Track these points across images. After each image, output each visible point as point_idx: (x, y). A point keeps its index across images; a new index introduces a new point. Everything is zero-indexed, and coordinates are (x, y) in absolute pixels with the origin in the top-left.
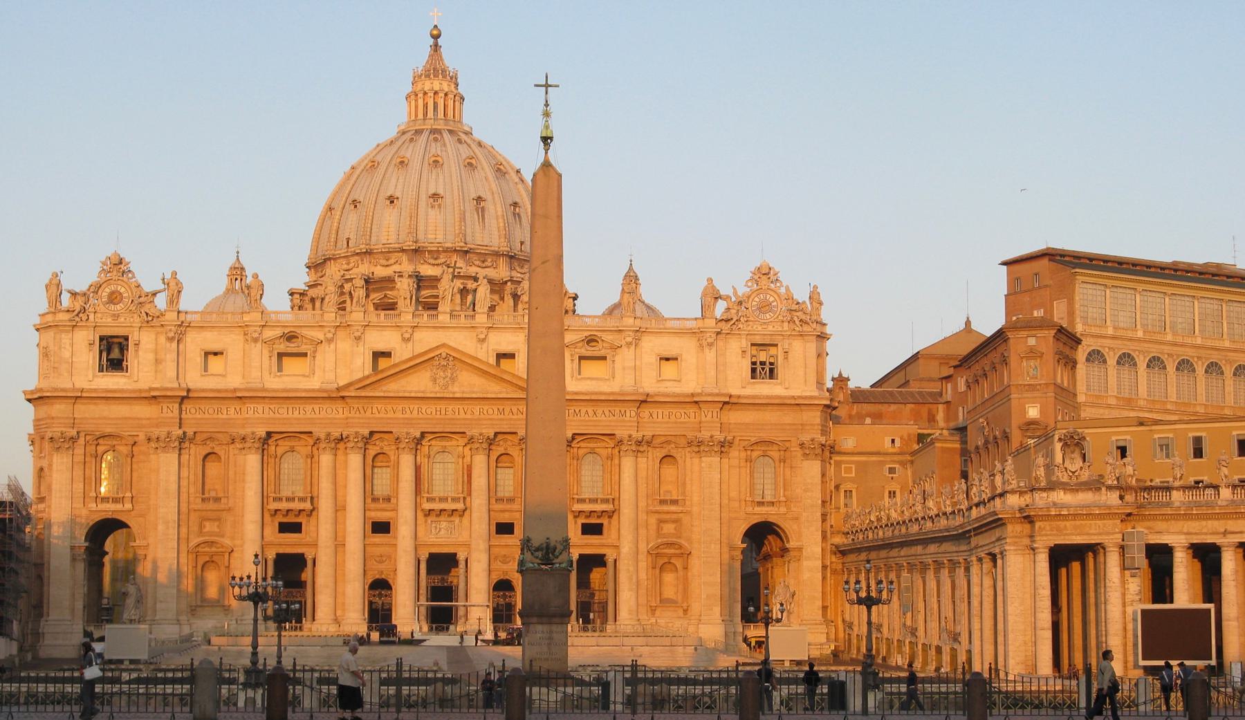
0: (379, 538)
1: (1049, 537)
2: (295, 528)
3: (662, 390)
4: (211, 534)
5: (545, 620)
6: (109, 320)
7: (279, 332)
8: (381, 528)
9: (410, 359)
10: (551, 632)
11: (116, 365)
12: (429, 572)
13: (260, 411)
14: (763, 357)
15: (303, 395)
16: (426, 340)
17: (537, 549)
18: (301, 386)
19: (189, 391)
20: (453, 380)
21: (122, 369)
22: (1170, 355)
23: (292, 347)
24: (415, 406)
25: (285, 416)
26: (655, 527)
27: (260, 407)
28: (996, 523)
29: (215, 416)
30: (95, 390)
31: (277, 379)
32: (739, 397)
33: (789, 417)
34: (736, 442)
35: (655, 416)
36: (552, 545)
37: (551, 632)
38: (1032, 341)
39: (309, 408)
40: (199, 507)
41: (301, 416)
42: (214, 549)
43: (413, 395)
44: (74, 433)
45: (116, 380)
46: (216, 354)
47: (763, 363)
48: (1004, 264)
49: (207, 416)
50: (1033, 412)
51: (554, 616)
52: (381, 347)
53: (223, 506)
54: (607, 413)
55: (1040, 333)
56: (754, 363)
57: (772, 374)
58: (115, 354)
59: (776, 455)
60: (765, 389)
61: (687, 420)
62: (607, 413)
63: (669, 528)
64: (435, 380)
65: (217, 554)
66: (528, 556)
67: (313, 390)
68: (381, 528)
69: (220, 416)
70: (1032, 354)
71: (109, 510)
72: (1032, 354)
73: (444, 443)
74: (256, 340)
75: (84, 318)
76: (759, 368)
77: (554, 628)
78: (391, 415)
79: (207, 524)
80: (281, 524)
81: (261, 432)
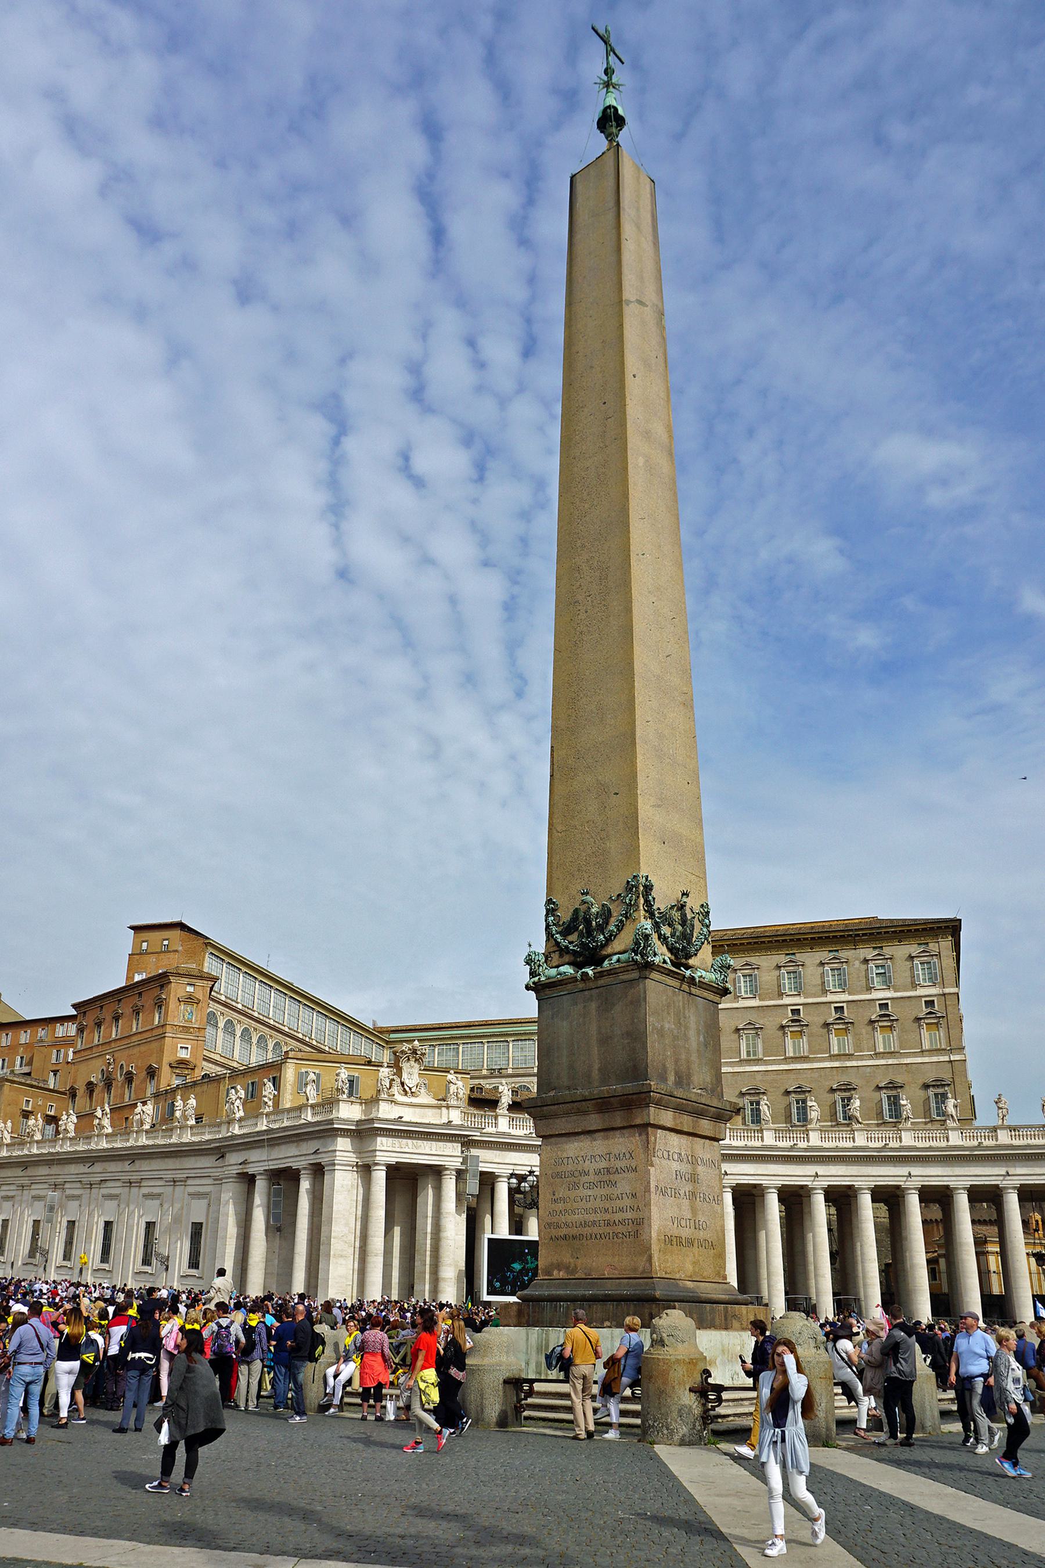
1: (389, 1151)
22: (255, 1029)
28: (327, 1132)
37: (693, 1161)
38: (190, 989)
48: (132, 928)
50: (183, 1055)
55: (199, 983)
70: (190, 1000)
72: (190, 1000)
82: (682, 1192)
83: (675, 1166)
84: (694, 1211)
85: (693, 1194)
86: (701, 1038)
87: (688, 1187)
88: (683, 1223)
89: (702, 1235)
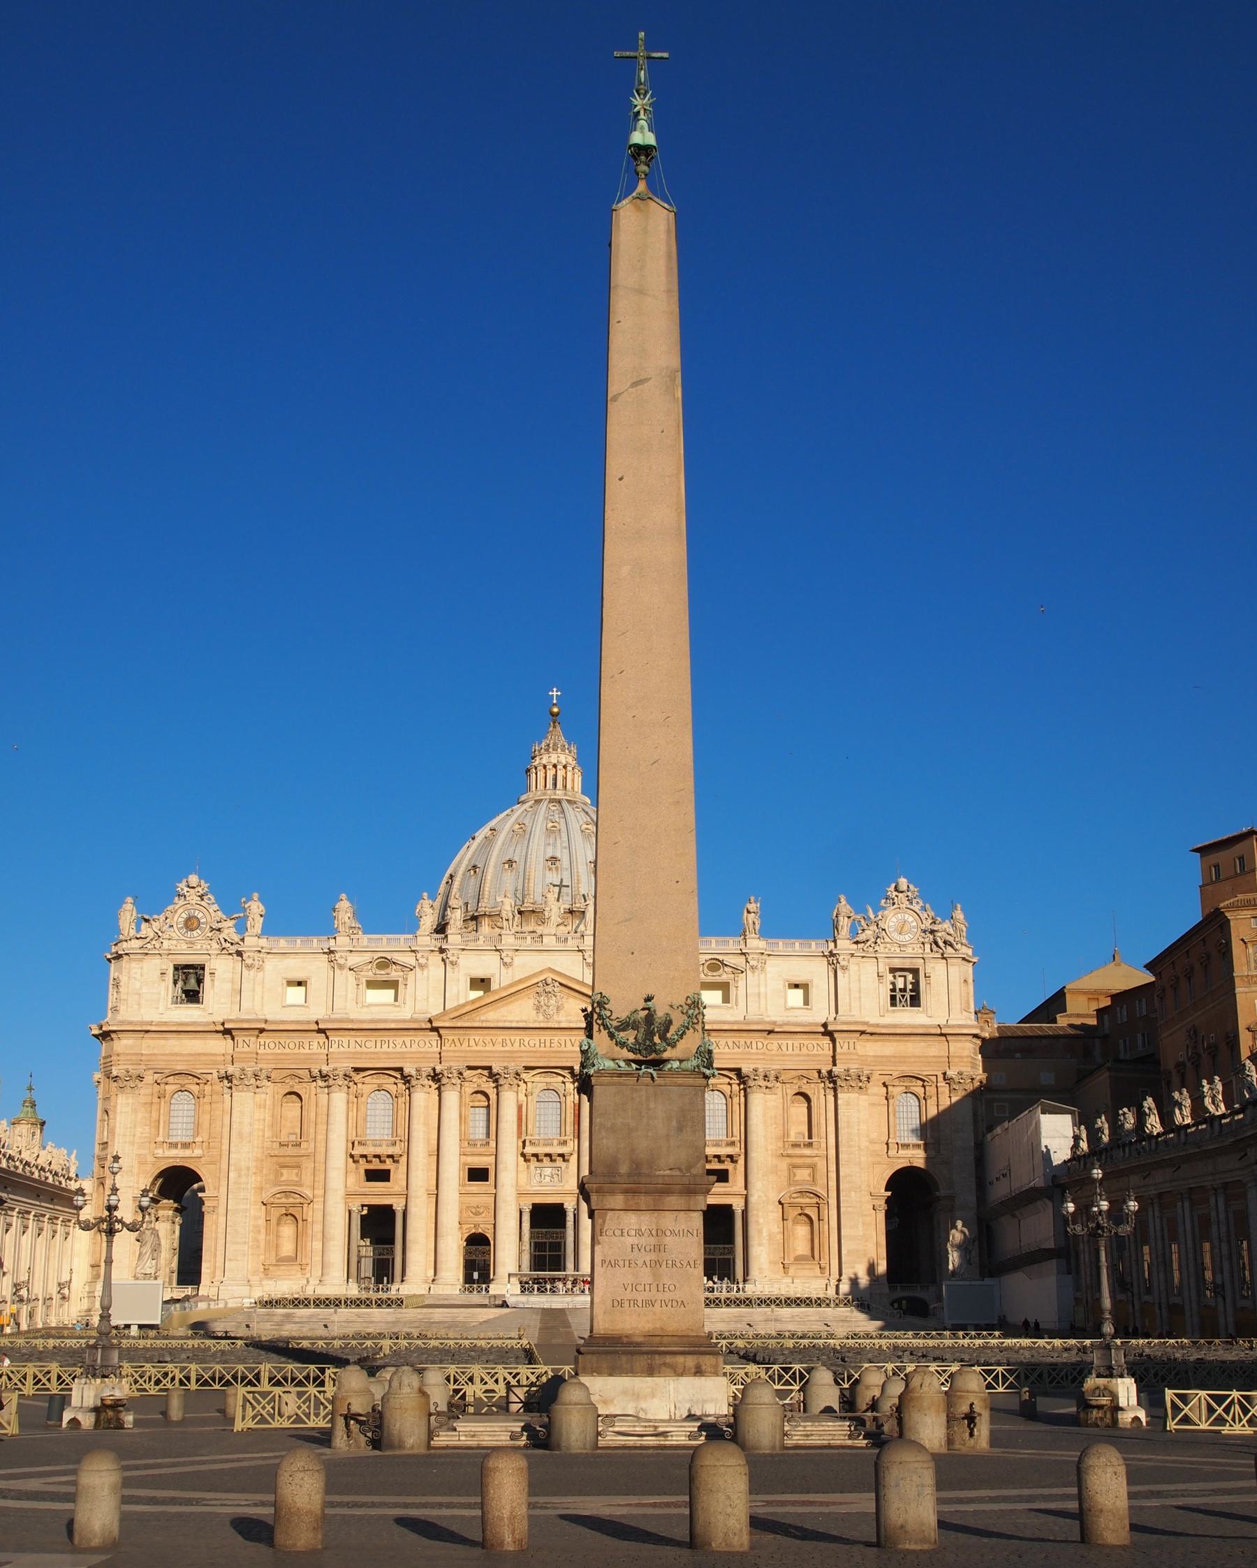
0: (477, 1186)
2: (383, 1176)
3: (792, 1019)
4: (288, 1183)
5: (643, 1200)
6: (185, 947)
7: (367, 957)
8: (478, 1174)
9: (511, 985)
10: (660, 1233)
11: (192, 996)
12: (532, 1226)
13: (346, 1045)
14: (900, 984)
15: (393, 1026)
16: (528, 964)
17: (625, 1026)
18: (391, 1016)
19: (266, 1021)
20: (558, 1009)
21: (198, 1002)
23: (382, 975)
24: (516, 1037)
25: (373, 1050)
26: (786, 1173)
27: (345, 1040)
29: (296, 1051)
30: (165, 1023)
31: (365, 1010)
32: (877, 1026)
33: (936, 1048)
34: (875, 1077)
35: (784, 1048)
36: (660, 1014)
37: (660, 1233)
39: (399, 1041)
40: (276, 1153)
41: (391, 1049)
42: (291, 1200)
43: (514, 1025)
44: (140, 1069)
45: (190, 1012)
46: (299, 984)
47: (903, 990)
49: (287, 1051)
51: (666, 1191)
52: (480, 973)
53: (302, 1152)
54: (731, 1044)
56: (893, 990)
57: (915, 1001)
58: (192, 984)
59: (920, 1091)
60: (906, 1017)
61: (821, 1052)
62: (731, 1044)
63: (803, 1174)
64: (538, 1008)
65: (294, 1205)
66: (601, 1041)
67: (404, 1021)
68: (478, 1174)
69: (302, 1050)
71: (176, 1157)
73: (548, 1080)
74: (341, 967)
75: (158, 946)
76: (898, 996)
77: (668, 1221)
78: (489, 1048)
79: (285, 1171)
80: (367, 1171)
81: (346, 1065)
82: (640, 1262)
83: (630, 1241)
84: (656, 1276)
85: (658, 1263)
86: (674, 1123)
87: (653, 1256)
88: (641, 1288)
89: (667, 1296)
